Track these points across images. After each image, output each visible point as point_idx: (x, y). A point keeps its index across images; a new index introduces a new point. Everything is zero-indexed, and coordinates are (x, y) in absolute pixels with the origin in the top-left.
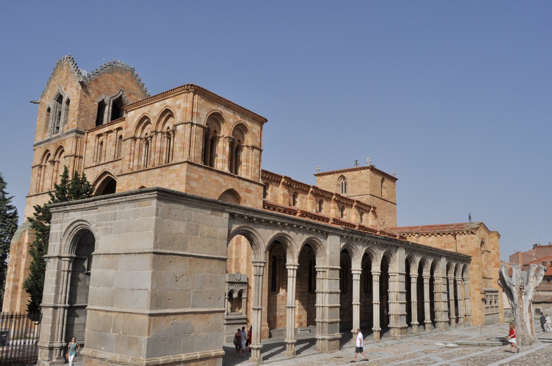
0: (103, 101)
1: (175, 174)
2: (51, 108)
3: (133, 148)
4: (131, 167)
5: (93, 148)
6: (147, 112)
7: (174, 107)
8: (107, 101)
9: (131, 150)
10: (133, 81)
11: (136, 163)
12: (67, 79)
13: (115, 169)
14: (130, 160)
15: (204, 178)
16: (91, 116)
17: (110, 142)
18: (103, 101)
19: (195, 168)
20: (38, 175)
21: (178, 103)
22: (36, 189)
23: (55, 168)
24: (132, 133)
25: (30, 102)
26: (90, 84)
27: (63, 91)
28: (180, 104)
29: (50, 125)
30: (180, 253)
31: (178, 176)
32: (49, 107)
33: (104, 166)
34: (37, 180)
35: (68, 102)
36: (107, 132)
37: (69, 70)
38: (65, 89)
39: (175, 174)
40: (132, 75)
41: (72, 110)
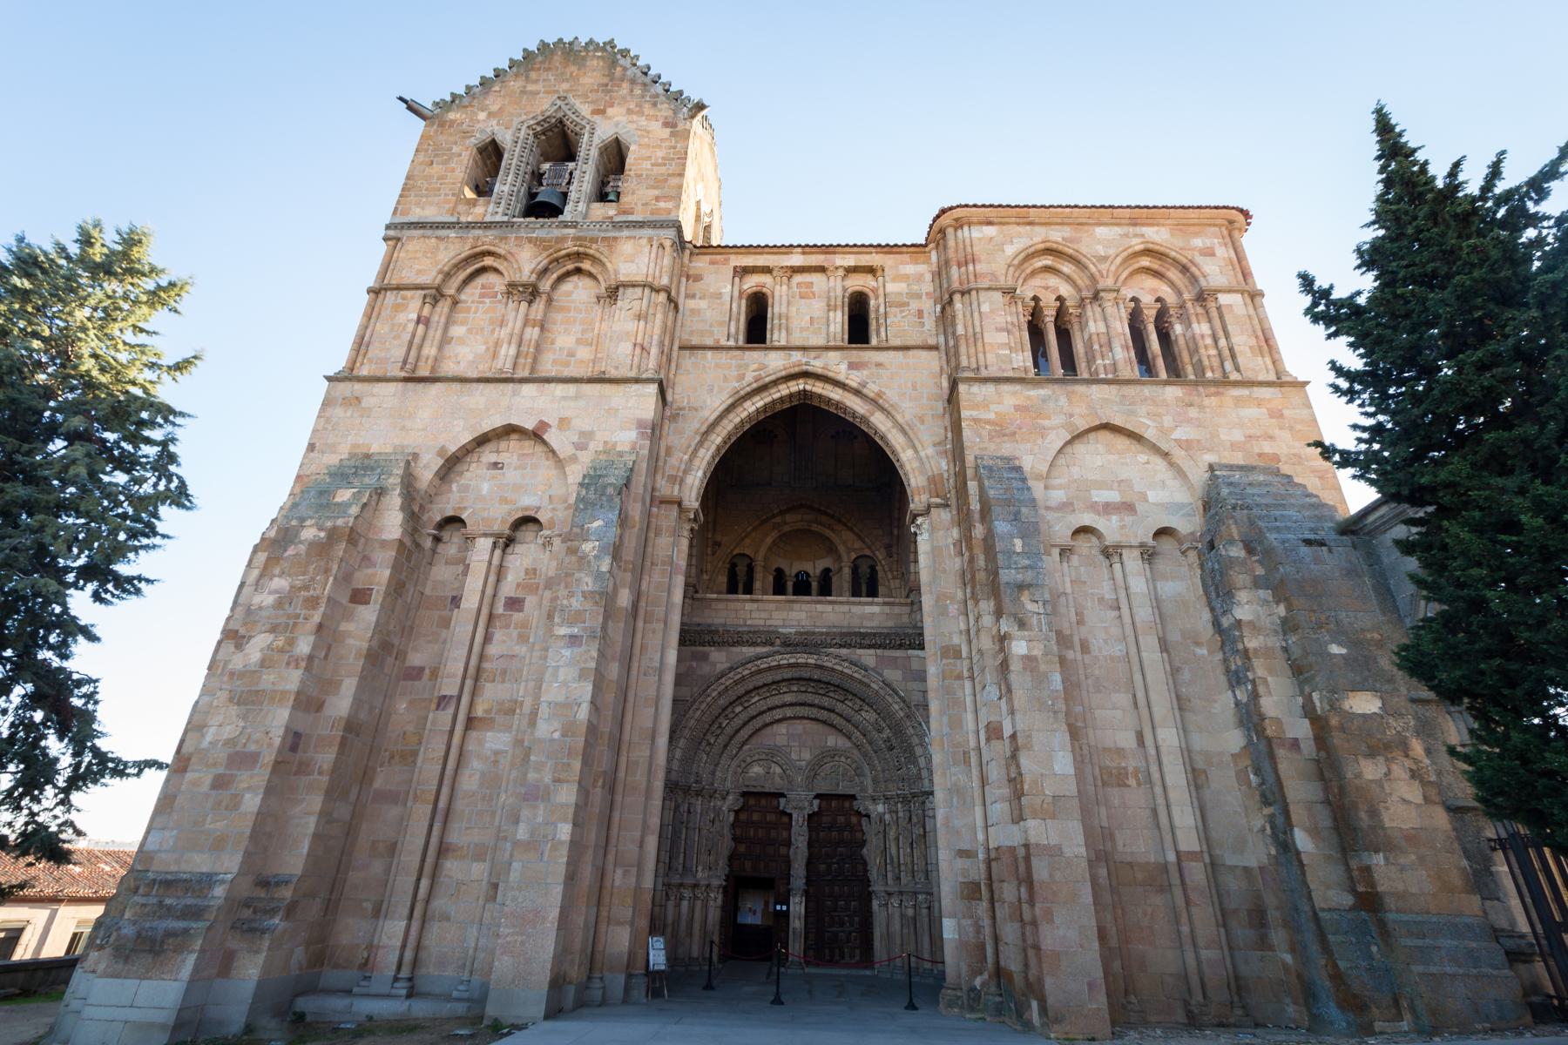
13: (865, 372)
17: (802, 297)
22: (405, 362)
25: (401, 99)
33: (797, 356)
34: (413, 335)
36: (792, 267)
39: (1265, 410)
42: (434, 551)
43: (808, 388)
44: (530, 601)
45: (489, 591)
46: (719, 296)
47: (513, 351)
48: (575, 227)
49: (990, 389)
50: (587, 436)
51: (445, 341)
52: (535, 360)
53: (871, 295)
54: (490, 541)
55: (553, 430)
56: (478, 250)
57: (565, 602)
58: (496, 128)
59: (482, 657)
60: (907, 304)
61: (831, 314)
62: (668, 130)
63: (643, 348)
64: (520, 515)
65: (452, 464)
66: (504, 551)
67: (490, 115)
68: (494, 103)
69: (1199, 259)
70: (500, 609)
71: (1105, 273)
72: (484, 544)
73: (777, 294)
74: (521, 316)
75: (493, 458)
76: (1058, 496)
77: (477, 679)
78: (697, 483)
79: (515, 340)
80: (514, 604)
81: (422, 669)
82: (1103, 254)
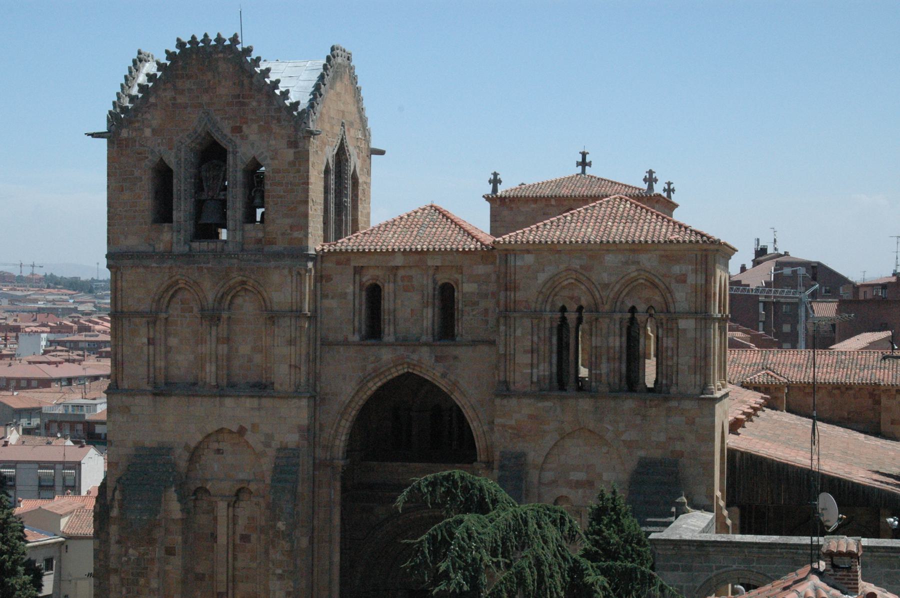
0: (328, 163)
1: (684, 418)
2: (173, 166)
3: (535, 339)
4: (535, 379)
5: (350, 297)
6: (578, 267)
7: (664, 276)
9: (532, 341)
11: (544, 371)
12: (243, 104)
20: (149, 339)
21: (677, 269)
22: (148, 377)
24: (533, 305)
25: (89, 135)
27: (230, 135)
28: (685, 275)
29: (176, 215)
31: (691, 422)
32: (161, 158)
33: (401, 351)
34: (149, 355)
37: (246, 82)
38: (237, 130)
39: (684, 418)
41: (281, 197)
42: (195, 506)
43: (411, 371)
44: (254, 537)
45: (231, 533)
46: (344, 295)
47: (214, 369)
48: (238, 259)
49: (514, 402)
50: (270, 437)
51: (168, 350)
53: (455, 287)
54: (226, 503)
55: (249, 433)
56: (173, 279)
57: (274, 556)
58: (162, 148)
59: (234, 568)
60: (476, 304)
61: (425, 310)
62: (292, 151)
63: (296, 367)
64: (238, 486)
65: (195, 454)
66: (234, 507)
67: (155, 132)
68: (155, 118)
69: (674, 286)
70: (238, 541)
71: (605, 299)
72: (222, 506)
73: (386, 290)
74: (214, 338)
75: (215, 446)
76: (548, 476)
77: (234, 581)
78: (342, 444)
79: (213, 359)
80: (245, 538)
81: (204, 575)
82: (607, 282)
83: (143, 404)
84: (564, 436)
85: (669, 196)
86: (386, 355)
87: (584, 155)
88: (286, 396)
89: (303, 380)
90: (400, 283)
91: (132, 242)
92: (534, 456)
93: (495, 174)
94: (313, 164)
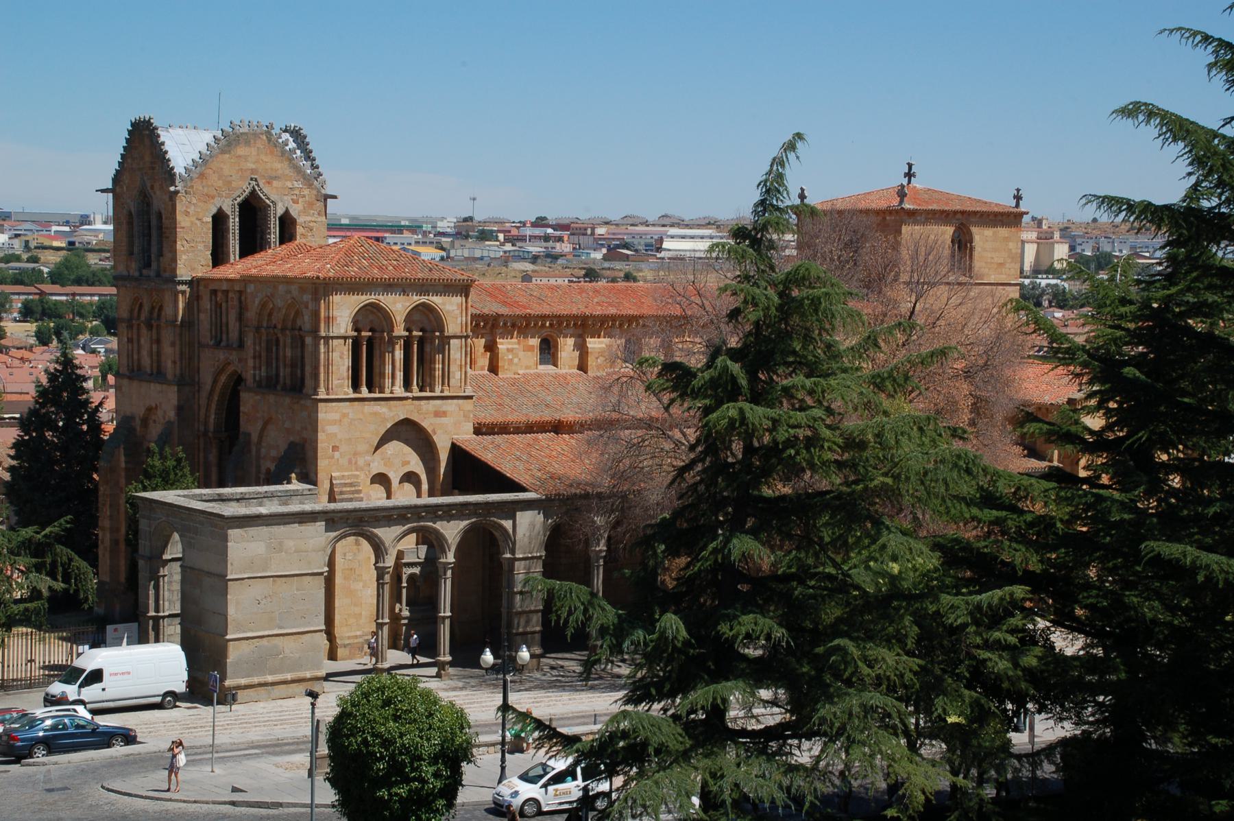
0: (221, 211)
3: (257, 348)
4: (257, 378)
8: (227, 209)
9: (255, 349)
10: (272, 153)
14: (254, 368)
15: (351, 416)
16: (201, 247)
18: (221, 211)
19: (334, 404)
23: (155, 337)
26: (192, 187)
29: (136, 250)
30: (259, 575)
35: (160, 215)
38: (152, 187)
40: (269, 140)
52: (159, 361)
65: (145, 421)
83: (125, 382)
84: (266, 423)
85: (1017, 205)
86: (221, 355)
87: (910, 166)
88: (169, 383)
89: (178, 372)
90: (230, 303)
91: (122, 270)
92: (254, 437)
93: (802, 190)
94: (187, 213)
